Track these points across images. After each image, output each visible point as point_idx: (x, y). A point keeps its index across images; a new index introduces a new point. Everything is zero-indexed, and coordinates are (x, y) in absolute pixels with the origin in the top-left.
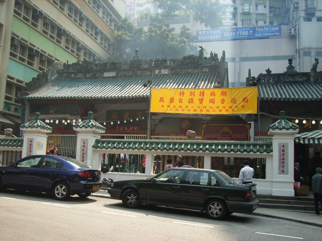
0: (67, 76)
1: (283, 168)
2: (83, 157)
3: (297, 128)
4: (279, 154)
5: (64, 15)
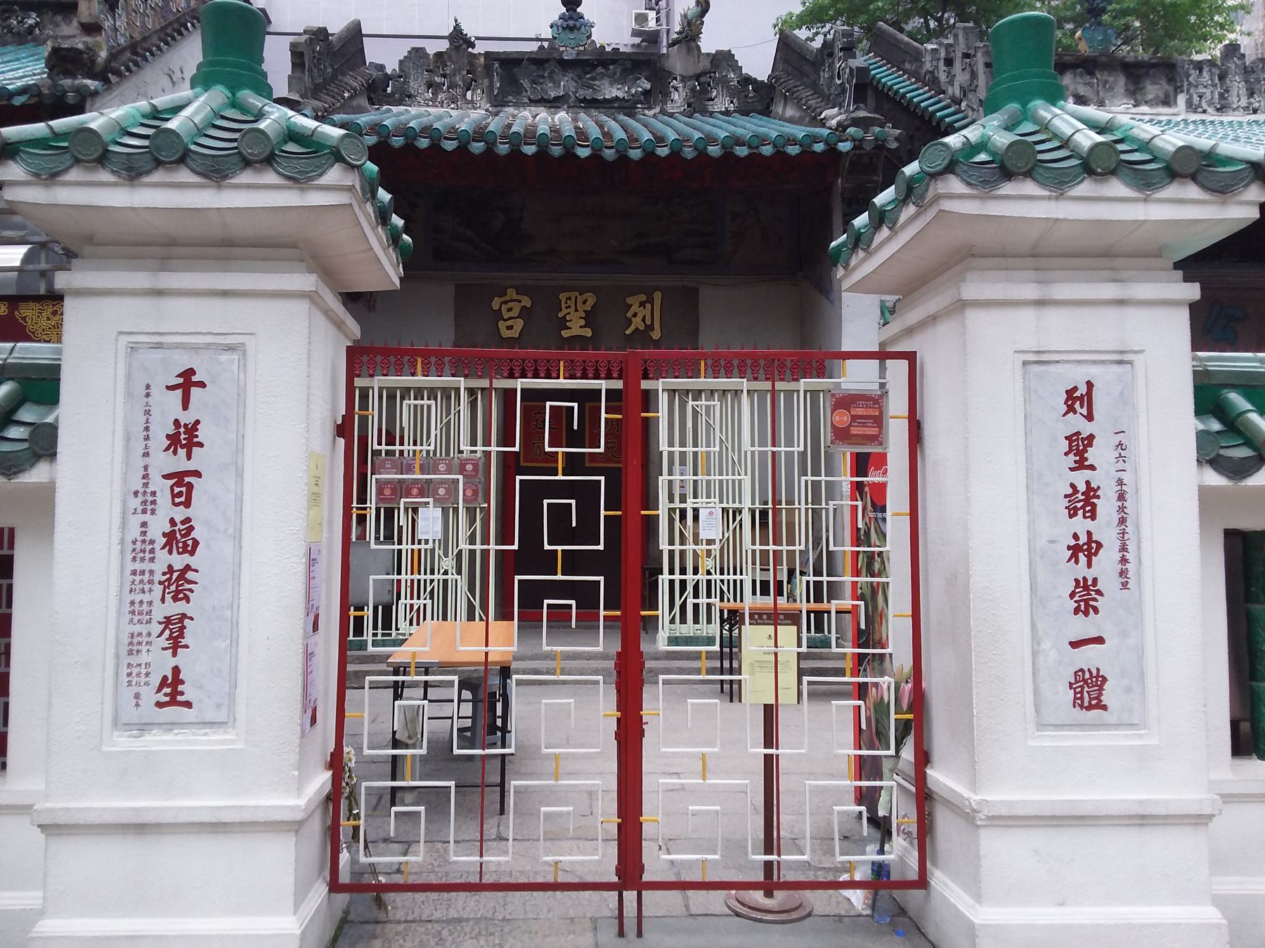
1: (176, 645)
4: (125, 479)
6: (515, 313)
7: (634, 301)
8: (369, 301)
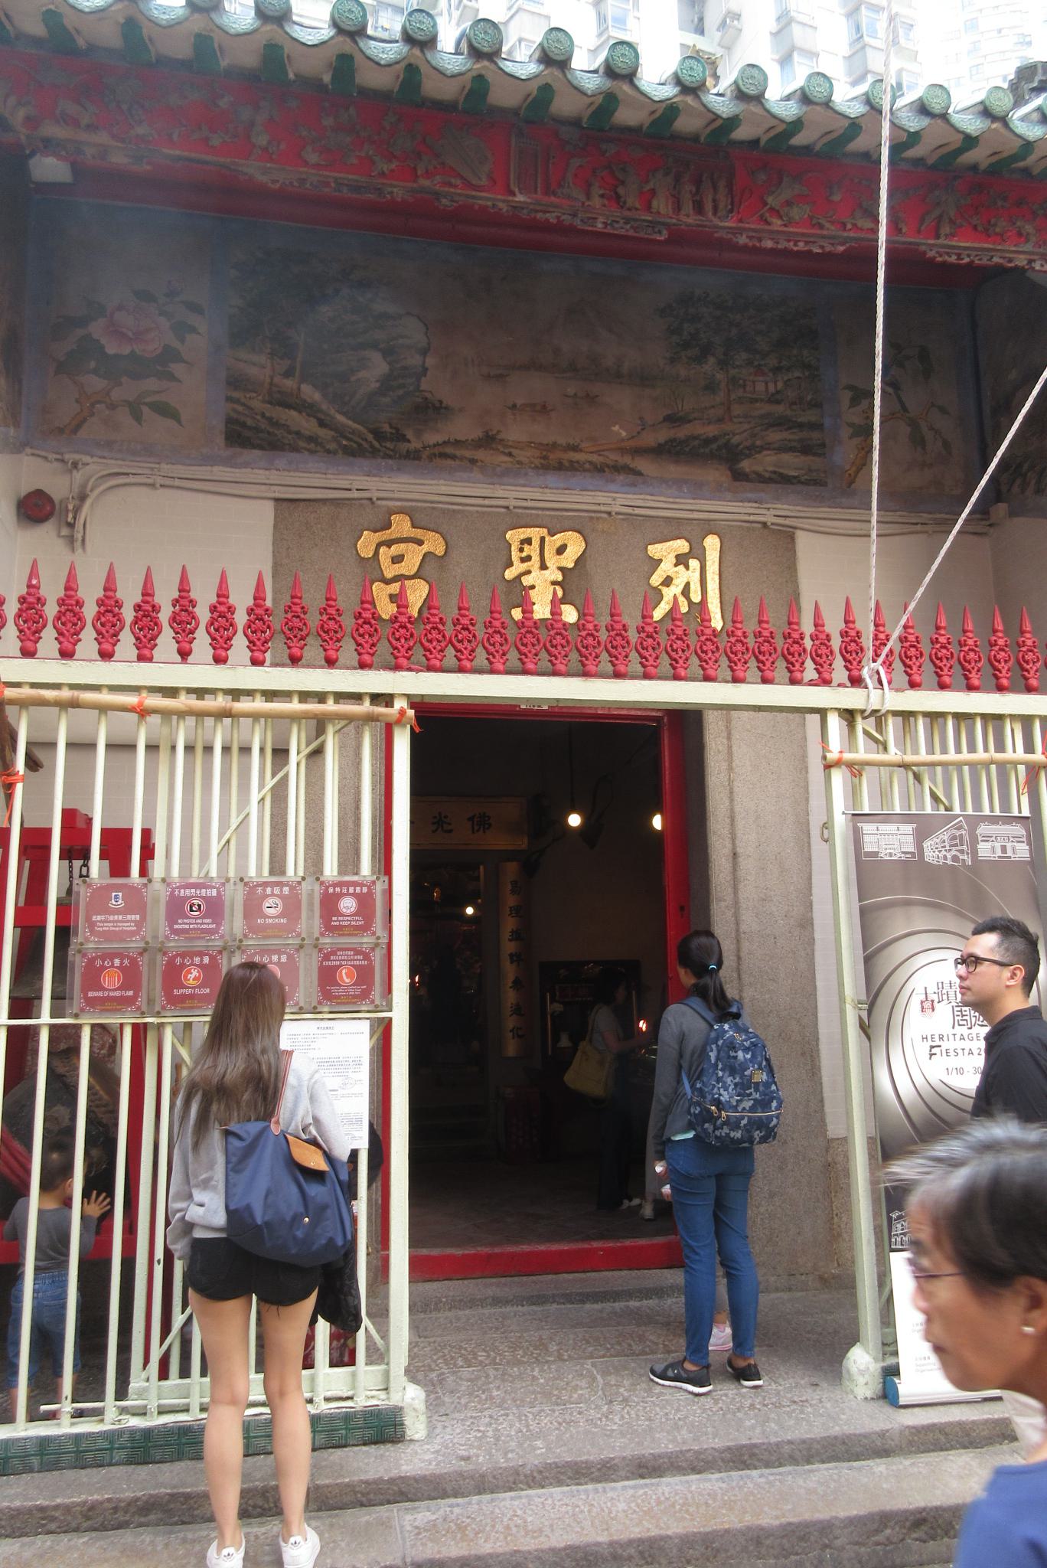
6: (410, 565)
7: (666, 551)
8: (71, 526)
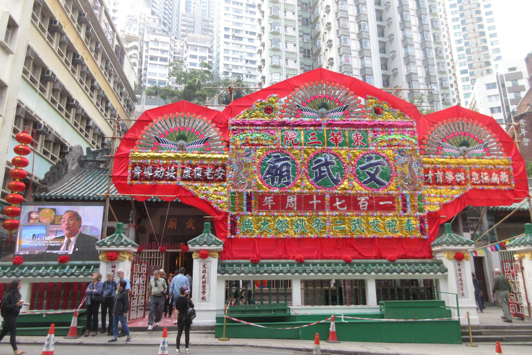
0: (92, 166)
1: (462, 290)
2: (204, 287)
3: (473, 243)
5: (74, 78)
